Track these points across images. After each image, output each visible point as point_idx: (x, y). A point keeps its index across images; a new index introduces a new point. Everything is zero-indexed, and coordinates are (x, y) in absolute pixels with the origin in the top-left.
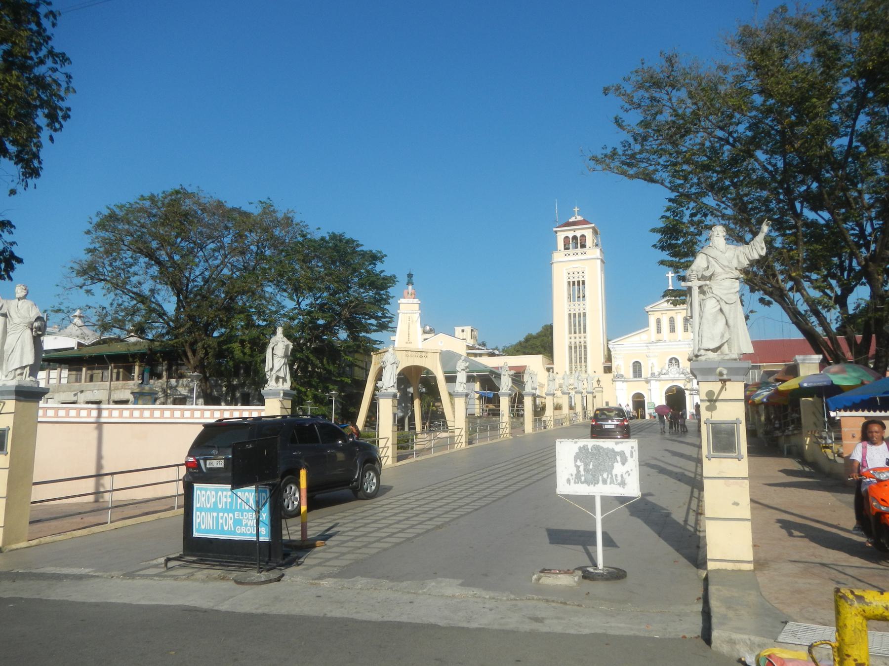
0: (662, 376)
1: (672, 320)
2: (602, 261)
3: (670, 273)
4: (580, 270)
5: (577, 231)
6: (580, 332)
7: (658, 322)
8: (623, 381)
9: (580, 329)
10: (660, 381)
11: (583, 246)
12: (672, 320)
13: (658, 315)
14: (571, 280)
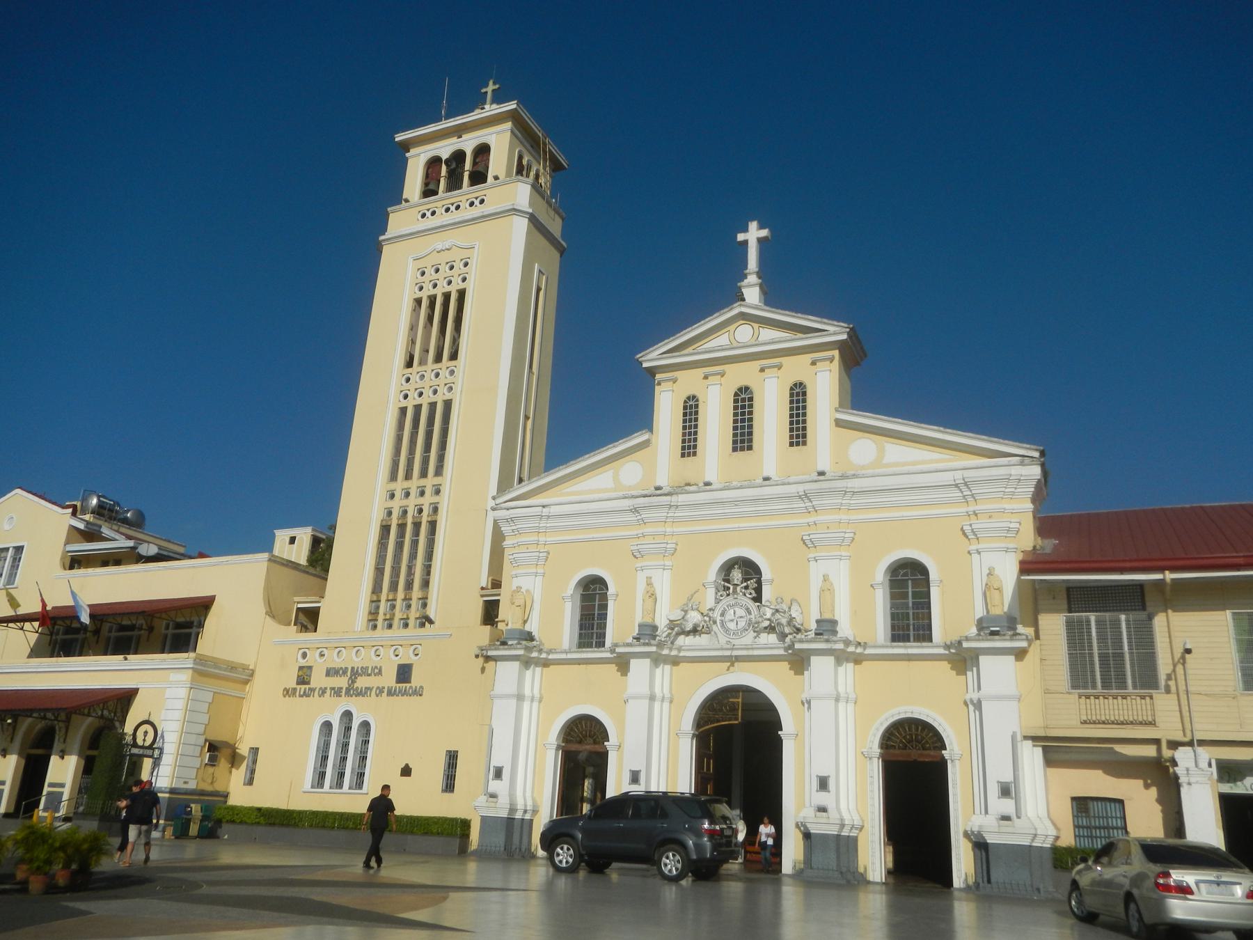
0: (681, 640)
1: (743, 402)
2: (533, 220)
3: (753, 226)
4: (456, 256)
5: (465, 137)
6: (424, 474)
7: (691, 410)
8: (527, 663)
9: (425, 461)
10: (675, 661)
11: (479, 177)
12: (743, 402)
13: (689, 382)
14: (429, 290)
